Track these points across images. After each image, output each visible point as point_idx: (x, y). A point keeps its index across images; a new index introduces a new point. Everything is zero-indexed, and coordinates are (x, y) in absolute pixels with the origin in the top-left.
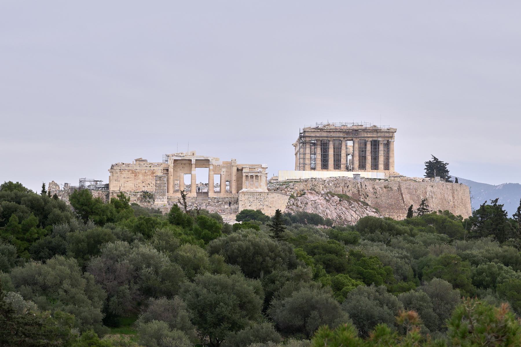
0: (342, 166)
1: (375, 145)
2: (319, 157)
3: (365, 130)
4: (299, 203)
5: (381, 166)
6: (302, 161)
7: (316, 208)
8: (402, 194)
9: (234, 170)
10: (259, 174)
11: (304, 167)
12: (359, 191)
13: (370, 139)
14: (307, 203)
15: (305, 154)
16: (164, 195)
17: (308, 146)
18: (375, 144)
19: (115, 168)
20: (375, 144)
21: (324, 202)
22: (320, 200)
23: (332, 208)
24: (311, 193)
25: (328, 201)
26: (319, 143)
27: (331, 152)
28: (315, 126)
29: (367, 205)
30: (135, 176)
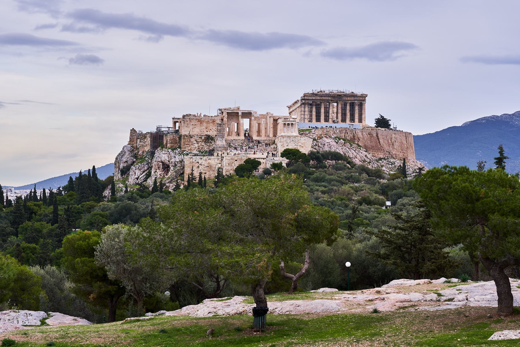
0: (330, 120)
2: (314, 113)
3: (346, 95)
4: (320, 144)
5: (357, 120)
6: (303, 116)
7: (330, 148)
8: (378, 139)
9: (272, 119)
10: (294, 123)
11: (304, 120)
12: (354, 136)
13: (350, 102)
14: (324, 145)
15: (305, 111)
16: (223, 138)
17: (307, 106)
18: (352, 105)
19: (186, 117)
20: (352, 105)
21: (335, 144)
22: (333, 143)
23: (340, 148)
25: (337, 143)
26: (314, 104)
27: (323, 110)
28: (311, 92)
29: (360, 146)
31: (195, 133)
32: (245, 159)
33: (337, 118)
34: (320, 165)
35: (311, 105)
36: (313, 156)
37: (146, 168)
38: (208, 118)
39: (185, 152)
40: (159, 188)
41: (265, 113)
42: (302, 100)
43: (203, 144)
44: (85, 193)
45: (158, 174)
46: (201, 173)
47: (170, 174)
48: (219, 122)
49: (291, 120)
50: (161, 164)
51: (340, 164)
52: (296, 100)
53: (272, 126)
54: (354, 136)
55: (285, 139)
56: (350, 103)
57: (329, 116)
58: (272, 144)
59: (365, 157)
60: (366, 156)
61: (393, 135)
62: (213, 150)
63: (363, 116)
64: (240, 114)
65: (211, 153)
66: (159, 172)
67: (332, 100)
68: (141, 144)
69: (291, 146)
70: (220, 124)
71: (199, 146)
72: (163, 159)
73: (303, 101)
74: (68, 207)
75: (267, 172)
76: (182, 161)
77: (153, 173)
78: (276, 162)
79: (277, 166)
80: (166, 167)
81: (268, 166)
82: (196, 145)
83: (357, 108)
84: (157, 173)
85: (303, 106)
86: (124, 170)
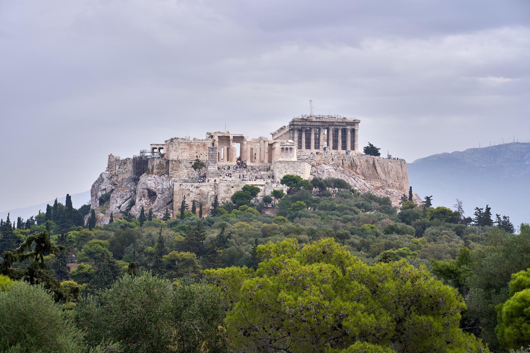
0: (321, 147)
1: (343, 132)
2: (304, 140)
4: (319, 172)
7: (329, 175)
13: (341, 128)
14: (323, 172)
18: (344, 131)
19: (174, 141)
20: (344, 131)
21: (334, 171)
24: (324, 163)
26: (304, 130)
27: (313, 137)
28: (301, 117)
30: (190, 147)
31: (185, 158)
32: (243, 185)
33: (328, 145)
34: (323, 193)
35: (300, 131)
36: (316, 182)
37: (128, 196)
38: (199, 141)
39: (173, 179)
40: (146, 218)
41: (257, 137)
42: (290, 125)
43: (193, 169)
44: (65, 222)
45: (144, 202)
46: (194, 202)
48: (210, 145)
49: (288, 144)
50: (147, 191)
51: (342, 192)
52: (282, 126)
53: (267, 151)
54: (352, 163)
55: (283, 165)
56: (342, 129)
57: (319, 143)
58: (267, 171)
59: (364, 186)
60: (365, 184)
61: (390, 163)
63: (356, 143)
64: (231, 138)
65: (203, 178)
66: (144, 201)
67: (322, 126)
68: (120, 170)
69: (290, 172)
70: (213, 149)
71: (188, 172)
72: (149, 186)
73: (292, 127)
74: (63, 235)
75: (267, 200)
76: (171, 189)
77: (137, 200)
78: (276, 189)
79: (277, 194)
80: (152, 195)
81: (268, 193)
82: (185, 171)
83: (349, 133)
84: (141, 203)
85: (292, 132)
86: (103, 198)
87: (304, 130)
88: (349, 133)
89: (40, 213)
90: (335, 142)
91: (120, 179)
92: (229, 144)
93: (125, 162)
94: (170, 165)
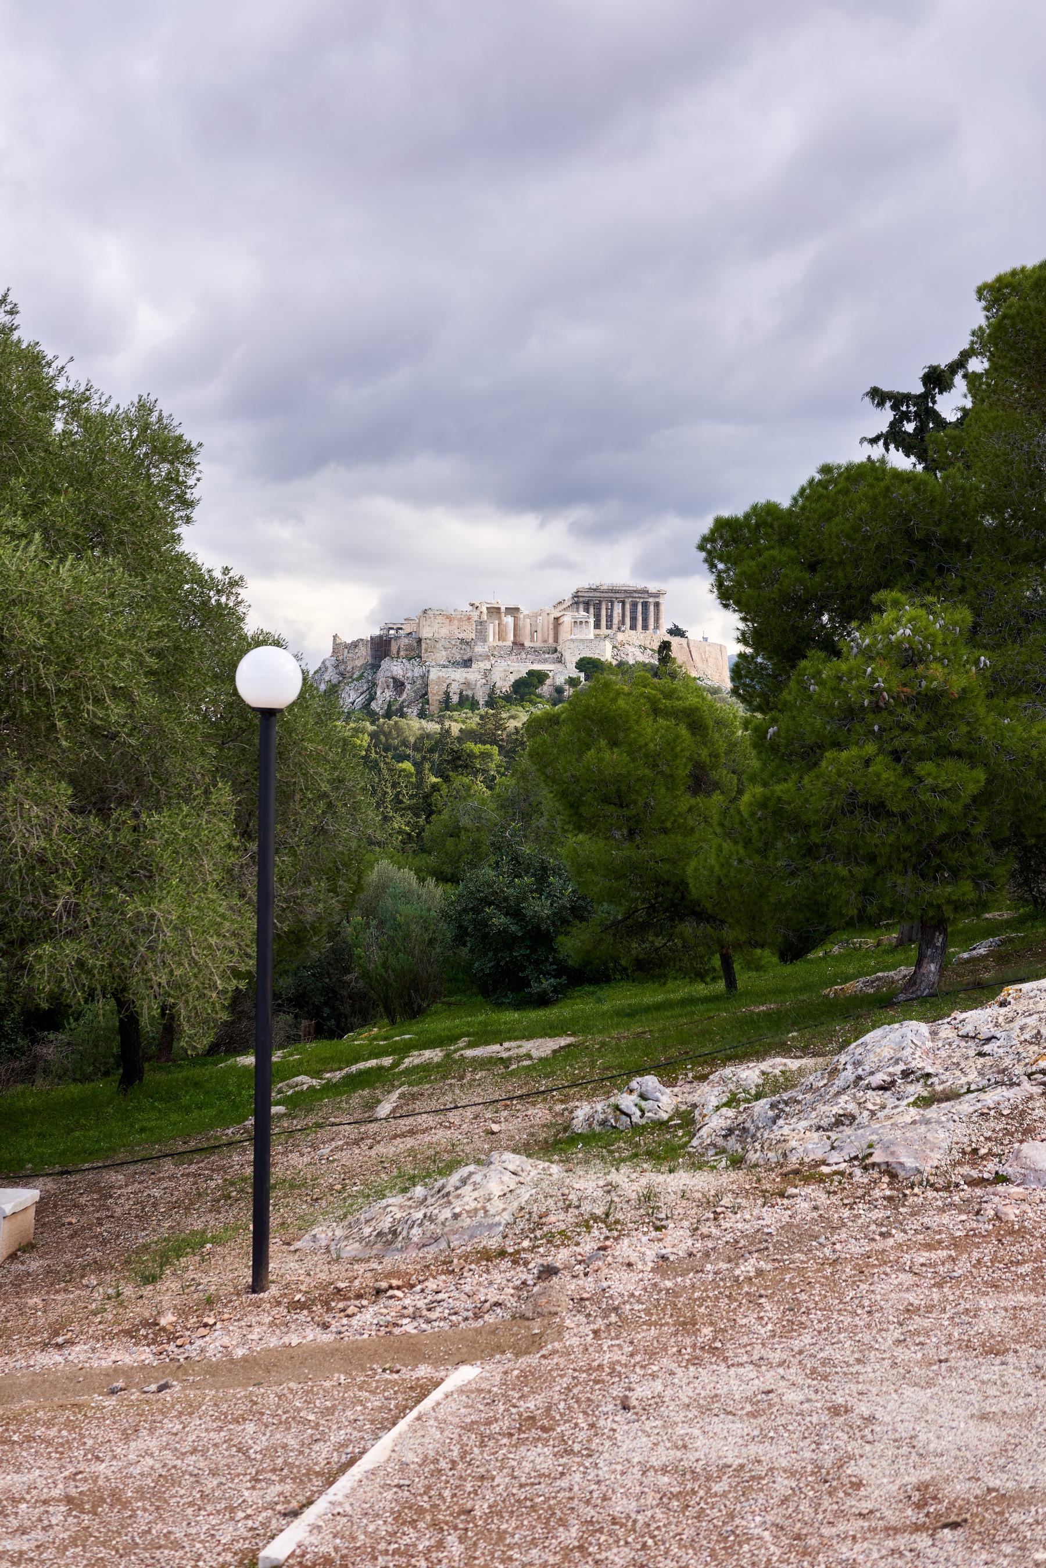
18: (645, 605)
27: (604, 612)
47: (404, 696)
62: (470, 660)
64: (503, 610)
65: (467, 663)
66: (389, 694)
76: (424, 677)
80: (399, 685)
83: (652, 608)
87: (593, 602)
88: (652, 608)
89: (261, 640)
90: (634, 619)
91: (349, 668)
92: (500, 618)
93: (355, 645)
94: (424, 646)
